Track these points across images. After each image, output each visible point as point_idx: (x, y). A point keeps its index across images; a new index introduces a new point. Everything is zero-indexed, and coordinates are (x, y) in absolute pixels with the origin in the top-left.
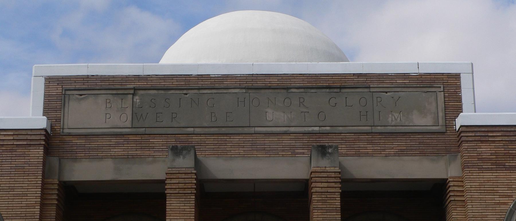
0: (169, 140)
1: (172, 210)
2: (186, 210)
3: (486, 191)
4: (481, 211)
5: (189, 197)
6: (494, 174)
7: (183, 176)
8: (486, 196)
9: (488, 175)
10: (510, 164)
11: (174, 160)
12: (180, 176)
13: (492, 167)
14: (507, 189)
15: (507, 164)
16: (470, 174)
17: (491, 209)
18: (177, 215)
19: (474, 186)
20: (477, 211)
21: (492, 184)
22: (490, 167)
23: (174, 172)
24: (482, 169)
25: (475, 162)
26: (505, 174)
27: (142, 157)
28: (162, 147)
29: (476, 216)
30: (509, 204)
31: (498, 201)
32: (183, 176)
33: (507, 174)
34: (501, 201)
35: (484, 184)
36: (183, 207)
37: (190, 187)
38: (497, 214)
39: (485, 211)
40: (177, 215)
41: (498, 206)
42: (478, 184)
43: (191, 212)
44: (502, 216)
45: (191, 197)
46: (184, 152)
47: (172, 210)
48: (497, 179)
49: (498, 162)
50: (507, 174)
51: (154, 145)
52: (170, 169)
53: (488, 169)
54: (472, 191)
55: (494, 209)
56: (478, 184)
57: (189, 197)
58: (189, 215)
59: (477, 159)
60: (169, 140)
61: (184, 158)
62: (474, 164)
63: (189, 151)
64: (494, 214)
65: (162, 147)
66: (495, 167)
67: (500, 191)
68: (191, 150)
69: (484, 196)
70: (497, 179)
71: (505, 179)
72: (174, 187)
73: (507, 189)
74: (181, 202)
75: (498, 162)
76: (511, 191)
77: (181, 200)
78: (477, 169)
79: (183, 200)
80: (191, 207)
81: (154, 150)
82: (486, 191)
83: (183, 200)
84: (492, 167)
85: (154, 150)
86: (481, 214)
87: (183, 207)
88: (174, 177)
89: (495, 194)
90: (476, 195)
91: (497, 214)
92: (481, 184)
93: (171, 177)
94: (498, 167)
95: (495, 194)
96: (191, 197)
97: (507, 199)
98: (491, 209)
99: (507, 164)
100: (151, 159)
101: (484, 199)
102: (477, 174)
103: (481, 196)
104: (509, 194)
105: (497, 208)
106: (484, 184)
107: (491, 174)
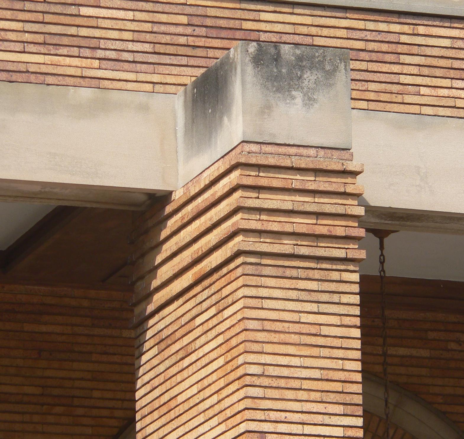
0: (164, 18)
1: (268, 325)
2: (325, 330)
5: (335, 276)
7: (311, 182)
11: (266, 109)
12: (297, 181)
18: (291, 350)
23: (271, 161)
27: (50, 79)
28: (131, 46)
32: (311, 182)
36: (311, 318)
37: (340, 232)
40: (291, 350)
43: (346, 343)
45: (347, 276)
46: (310, 77)
47: (268, 325)
51: (97, 33)
52: (254, 148)
57: (335, 276)
58: (340, 353)
60: (164, 18)
61: (309, 101)
63: (331, 74)
65: (131, 46)
68: (335, 69)
72: (275, 227)
74: (304, 296)
77: (302, 284)
79: (313, 285)
80: (347, 321)
81: (100, 54)
83: (313, 285)
85: (100, 54)
87: (311, 318)
88: (275, 183)
93: (263, 182)
96: (347, 276)
100: (86, 94)
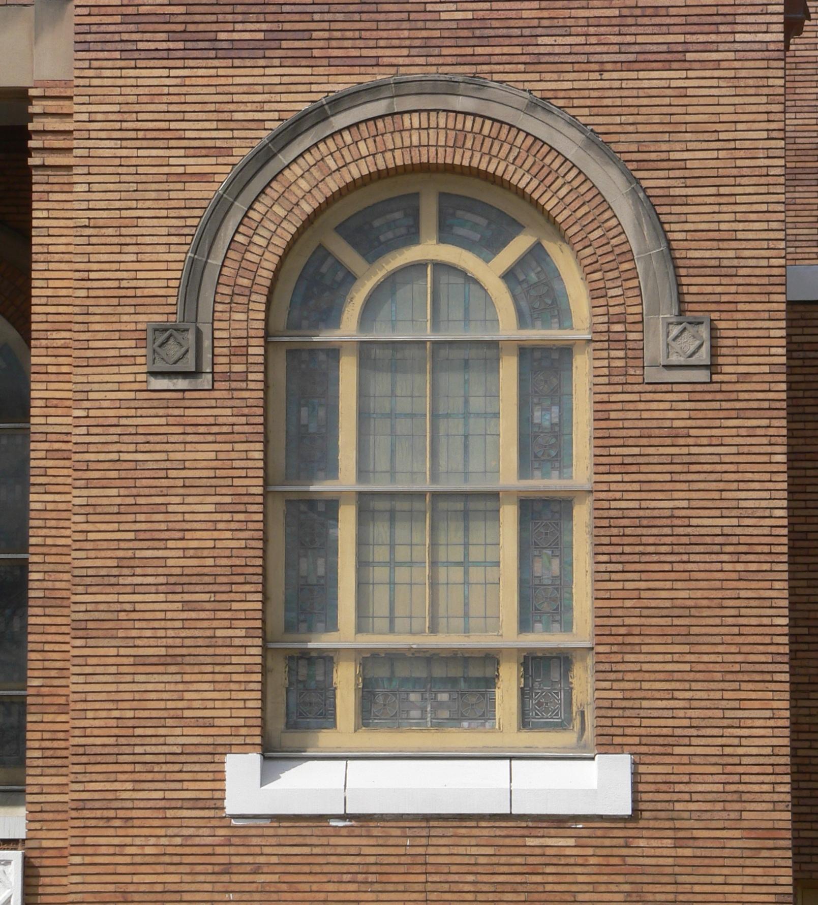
3: (141, 134)
4: (118, 205)
6: (174, 73)
8: (142, 153)
9: (153, 76)
10: (236, 36)
13: (171, 45)
14: (214, 125)
15: (222, 36)
16: (91, 73)
17: (153, 195)
19: (100, 117)
20: (103, 205)
21: (164, 107)
22: (164, 45)
24: (136, 55)
25: (112, 28)
26: (213, 72)
29: (101, 223)
30: (217, 178)
31: (181, 170)
33: (221, 72)
34: (190, 170)
35: (137, 108)
38: (172, 213)
39: (133, 204)
41: (180, 186)
42: (116, 108)
44: (190, 222)
48: (184, 90)
49: (191, 27)
50: (221, 72)
53: (154, 55)
54: (93, 135)
55: (165, 195)
56: (116, 108)
59: (118, 19)
62: (108, 37)
64: (164, 213)
66: (180, 45)
67: (189, 134)
69: (134, 152)
70: (184, 90)
71: (212, 90)
73: (214, 125)
75: (191, 27)
76: (228, 134)
78: (117, 55)
82: (141, 134)
84: (171, 45)
86: (116, 214)
89: (173, 143)
90: (107, 149)
91: (172, 213)
92: (125, 108)
94: (189, 45)
95: (173, 143)
97: (213, 160)
98: (153, 195)
99: (222, 36)
101: (134, 161)
102: (117, 73)
103: (124, 152)
104: (219, 143)
105: (173, 195)
106: (137, 108)
107: (165, 72)
